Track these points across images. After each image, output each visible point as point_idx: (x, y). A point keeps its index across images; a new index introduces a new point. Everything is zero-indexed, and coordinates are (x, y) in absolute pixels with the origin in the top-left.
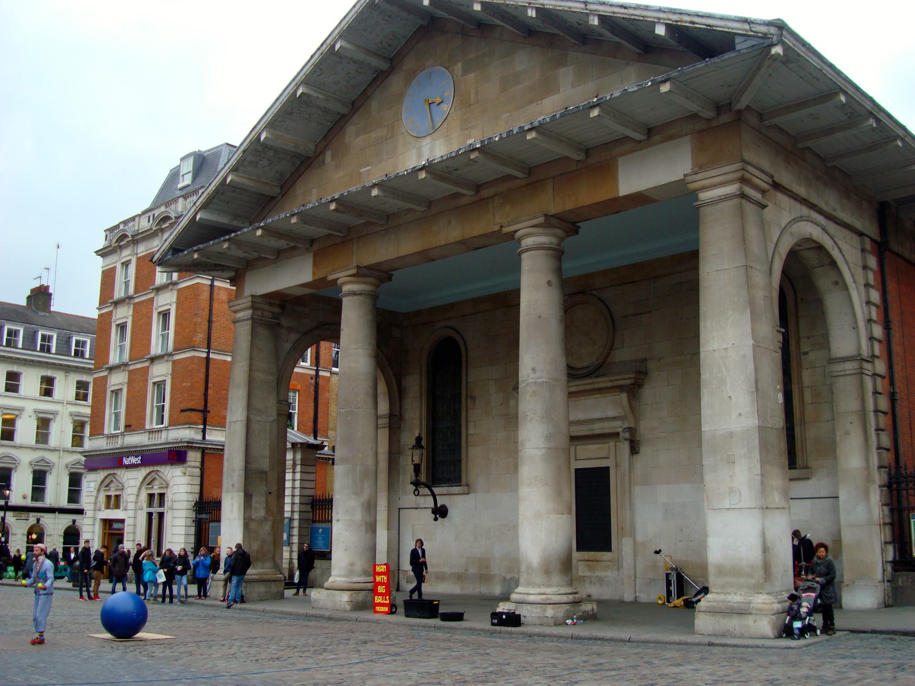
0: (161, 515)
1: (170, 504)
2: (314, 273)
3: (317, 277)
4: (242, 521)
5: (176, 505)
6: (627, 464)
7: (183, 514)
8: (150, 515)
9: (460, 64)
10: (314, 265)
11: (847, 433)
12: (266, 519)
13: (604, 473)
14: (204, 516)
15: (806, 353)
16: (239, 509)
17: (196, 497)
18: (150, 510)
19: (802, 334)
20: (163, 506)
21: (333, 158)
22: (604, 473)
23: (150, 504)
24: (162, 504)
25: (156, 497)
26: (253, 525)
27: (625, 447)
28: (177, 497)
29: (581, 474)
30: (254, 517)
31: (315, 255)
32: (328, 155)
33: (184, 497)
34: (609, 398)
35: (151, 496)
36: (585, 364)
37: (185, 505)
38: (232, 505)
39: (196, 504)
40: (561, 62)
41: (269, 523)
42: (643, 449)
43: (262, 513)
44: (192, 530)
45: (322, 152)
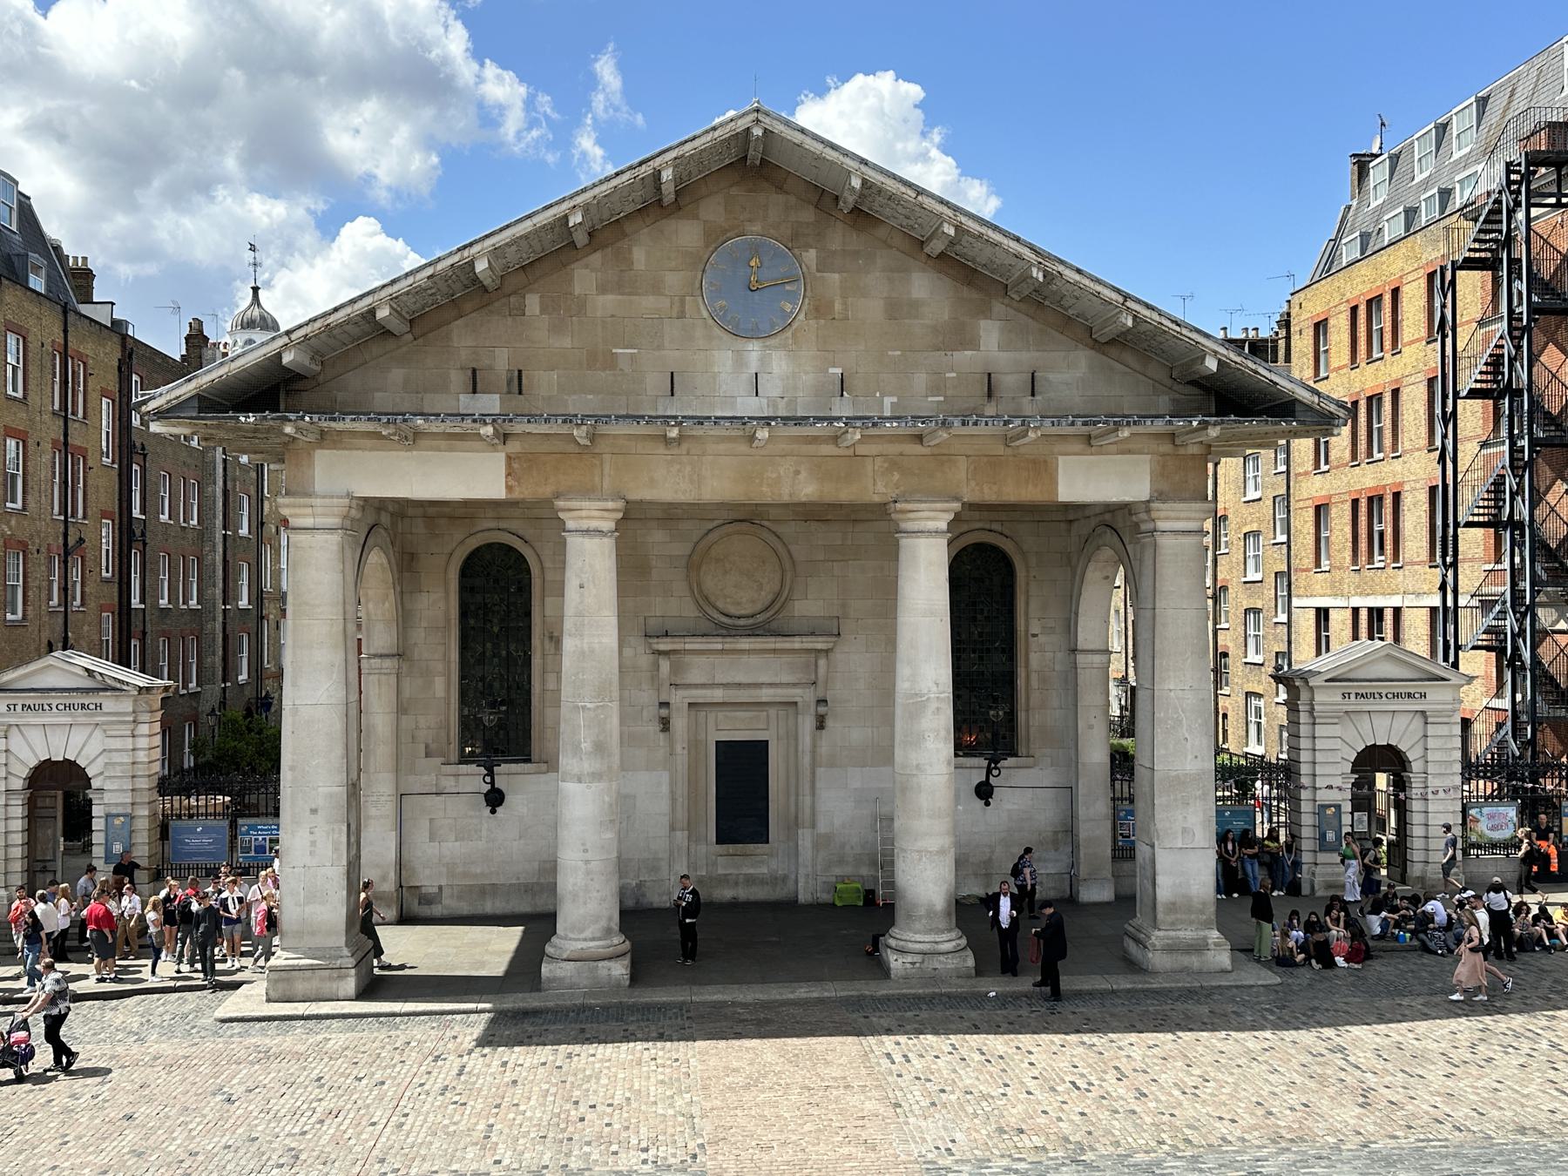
2: (509, 488)
3: (516, 495)
6: (808, 740)
9: (812, 253)
10: (508, 475)
11: (1091, 727)
13: (759, 750)
15: (1035, 635)
19: (1032, 614)
21: (543, 310)
22: (759, 750)
27: (807, 723)
29: (727, 751)
31: (509, 458)
32: (533, 303)
34: (786, 658)
36: (743, 612)
40: (985, 312)
42: (829, 723)
45: (520, 292)
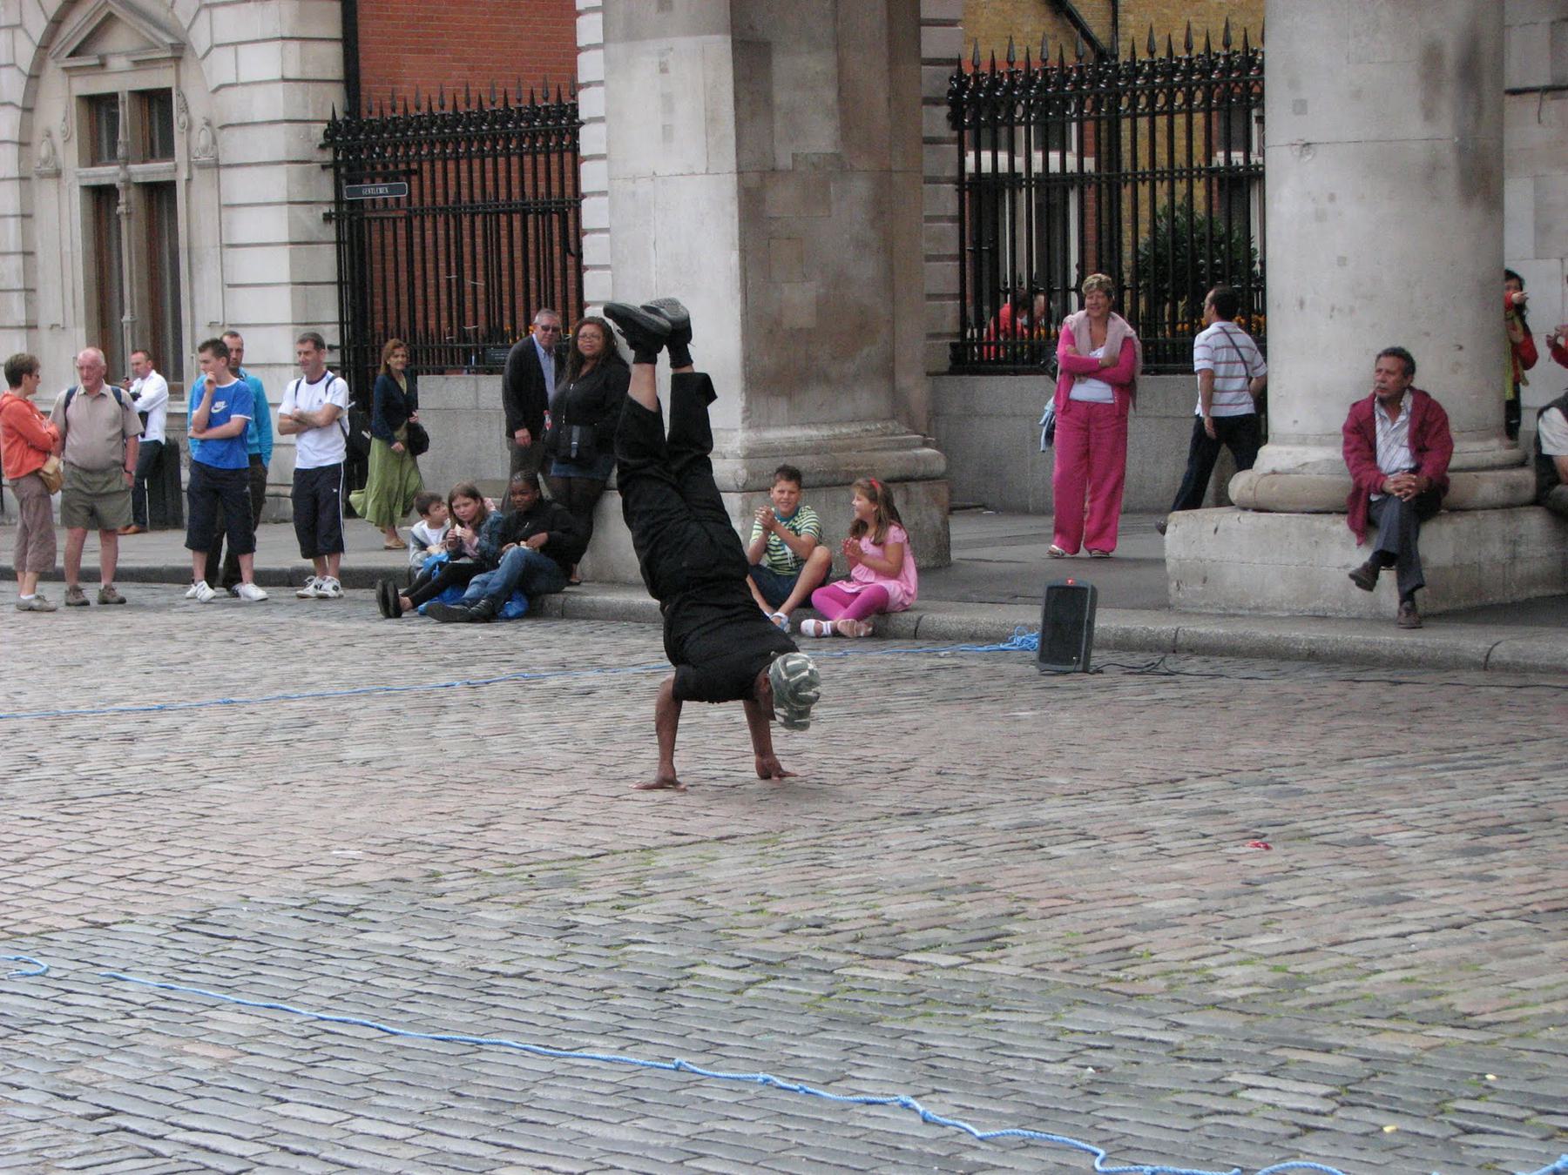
0: (160, 195)
1: (201, 139)
4: (728, 186)
5: (236, 146)
7: (277, 183)
8: (101, 197)
12: (838, 166)
14: (376, 191)
16: (712, 120)
17: (332, 101)
18: (106, 174)
20: (168, 151)
23: (99, 145)
24: (159, 142)
25: (124, 111)
26: (781, 198)
28: (235, 105)
30: (785, 161)
33: (271, 103)
35: (99, 107)
37: (278, 142)
38: (668, 101)
39: (335, 134)
41: (860, 188)
43: (821, 137)
44: (325, 262)
